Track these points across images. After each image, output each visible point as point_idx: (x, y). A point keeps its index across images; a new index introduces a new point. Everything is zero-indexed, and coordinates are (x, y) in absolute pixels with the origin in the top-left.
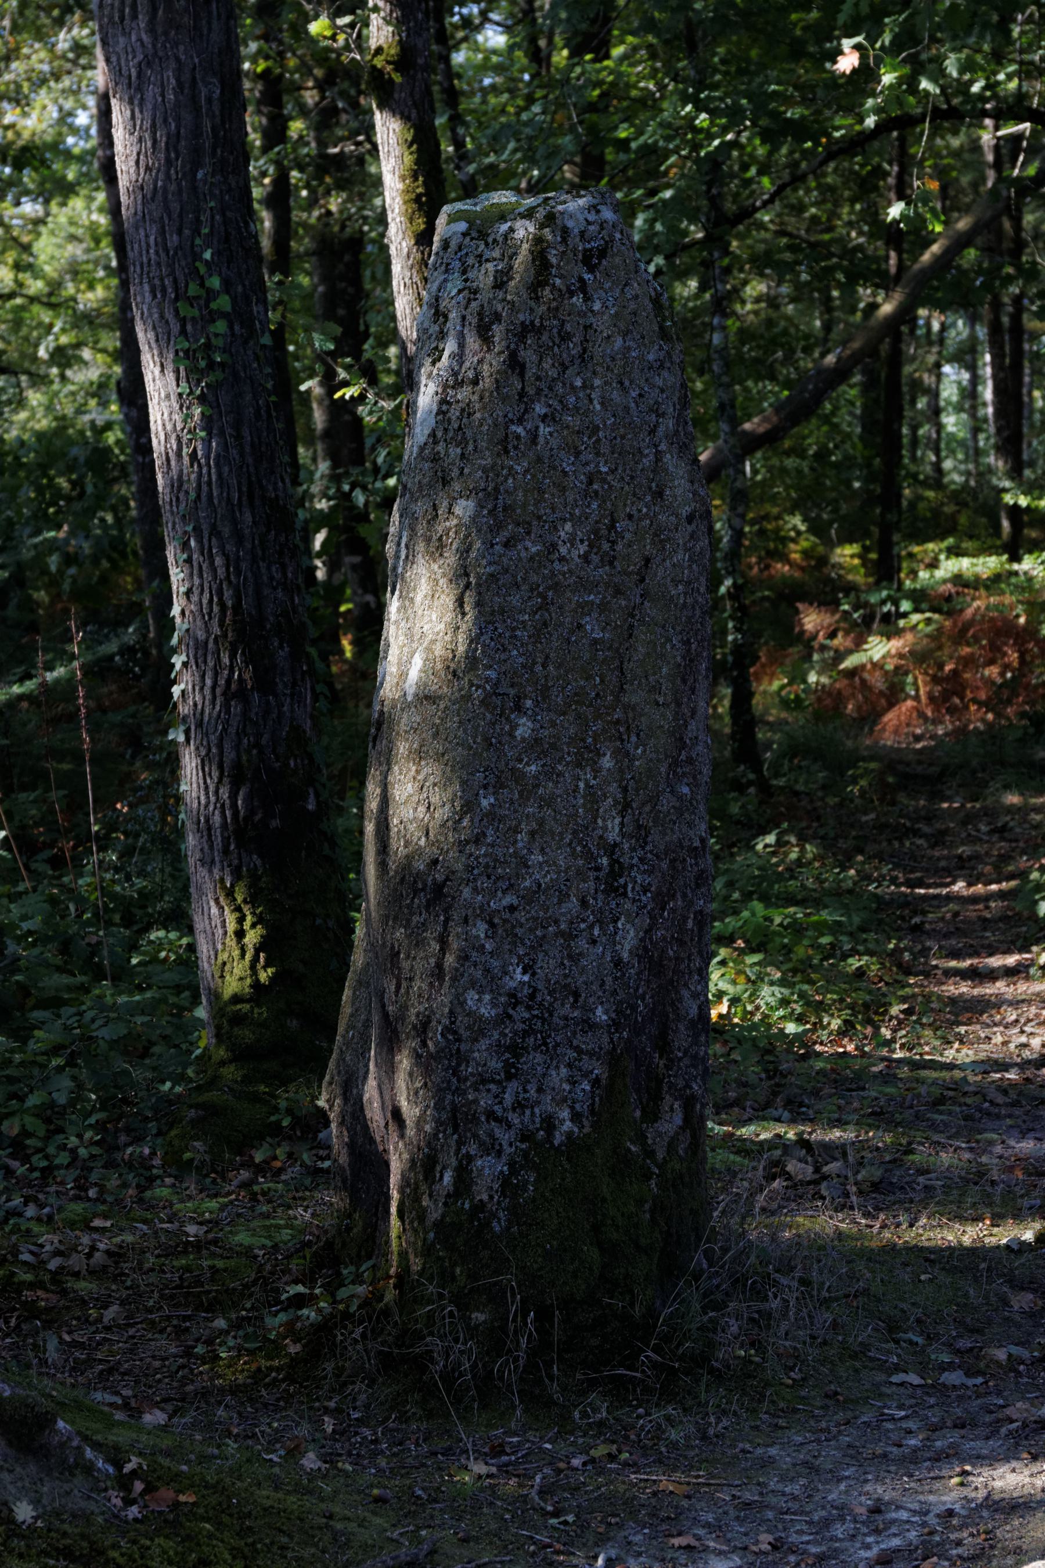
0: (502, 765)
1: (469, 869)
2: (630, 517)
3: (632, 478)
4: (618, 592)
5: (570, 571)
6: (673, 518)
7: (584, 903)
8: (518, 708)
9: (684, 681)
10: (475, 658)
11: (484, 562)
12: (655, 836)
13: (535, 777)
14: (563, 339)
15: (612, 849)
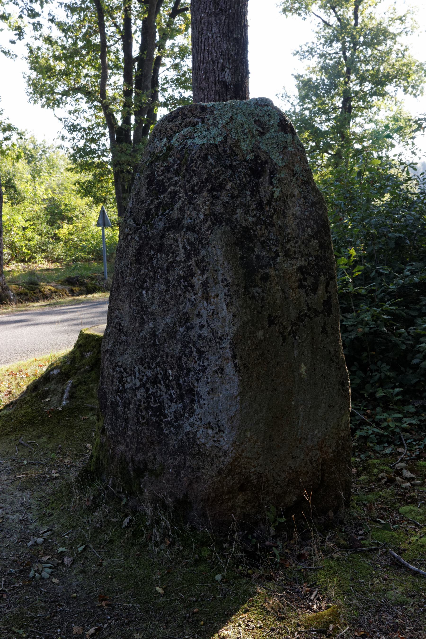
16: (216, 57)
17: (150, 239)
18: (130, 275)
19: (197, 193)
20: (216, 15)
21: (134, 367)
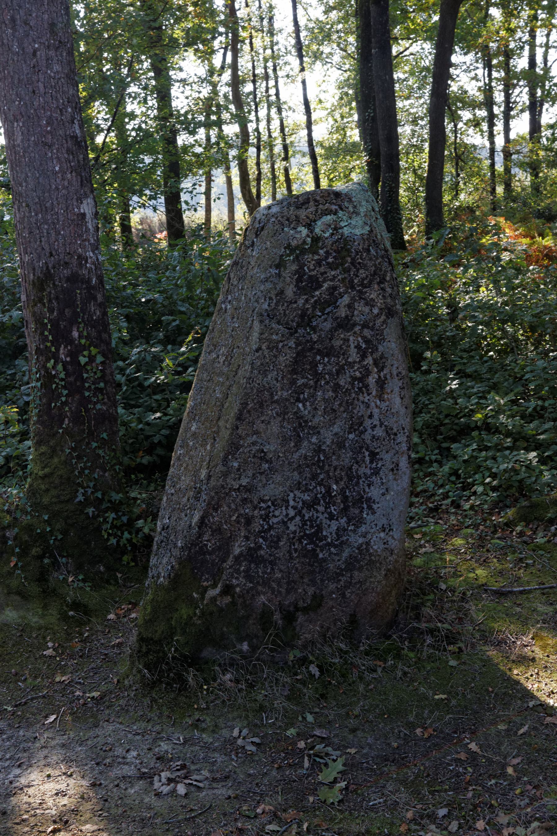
7: (188, 500)
8: (194, 419)
16: (63, 104)
17: (315, 342)
18: (282, 389)
19: (366, 287)
20: (57, 49)
21: (288, 495)
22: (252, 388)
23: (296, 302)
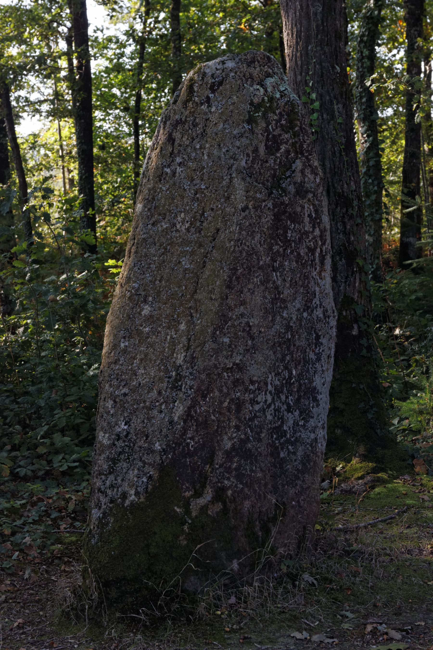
0: (133, 328)
1: (110, 375)
2: (212, 209)
3: (216, 191)
4: (201, 246)
5: (180, 236)
6: (233, 210)
7: (160, 393)
8: (145, 301)
9: (229, 287)
10: (130, 278)
11: (142, 233)
12: (200, 362)
13: (148, 334)
14: (194, 126)
15: (178, 368)
17: (287, 205)
22: (241, 252)
23: (267, 162)
